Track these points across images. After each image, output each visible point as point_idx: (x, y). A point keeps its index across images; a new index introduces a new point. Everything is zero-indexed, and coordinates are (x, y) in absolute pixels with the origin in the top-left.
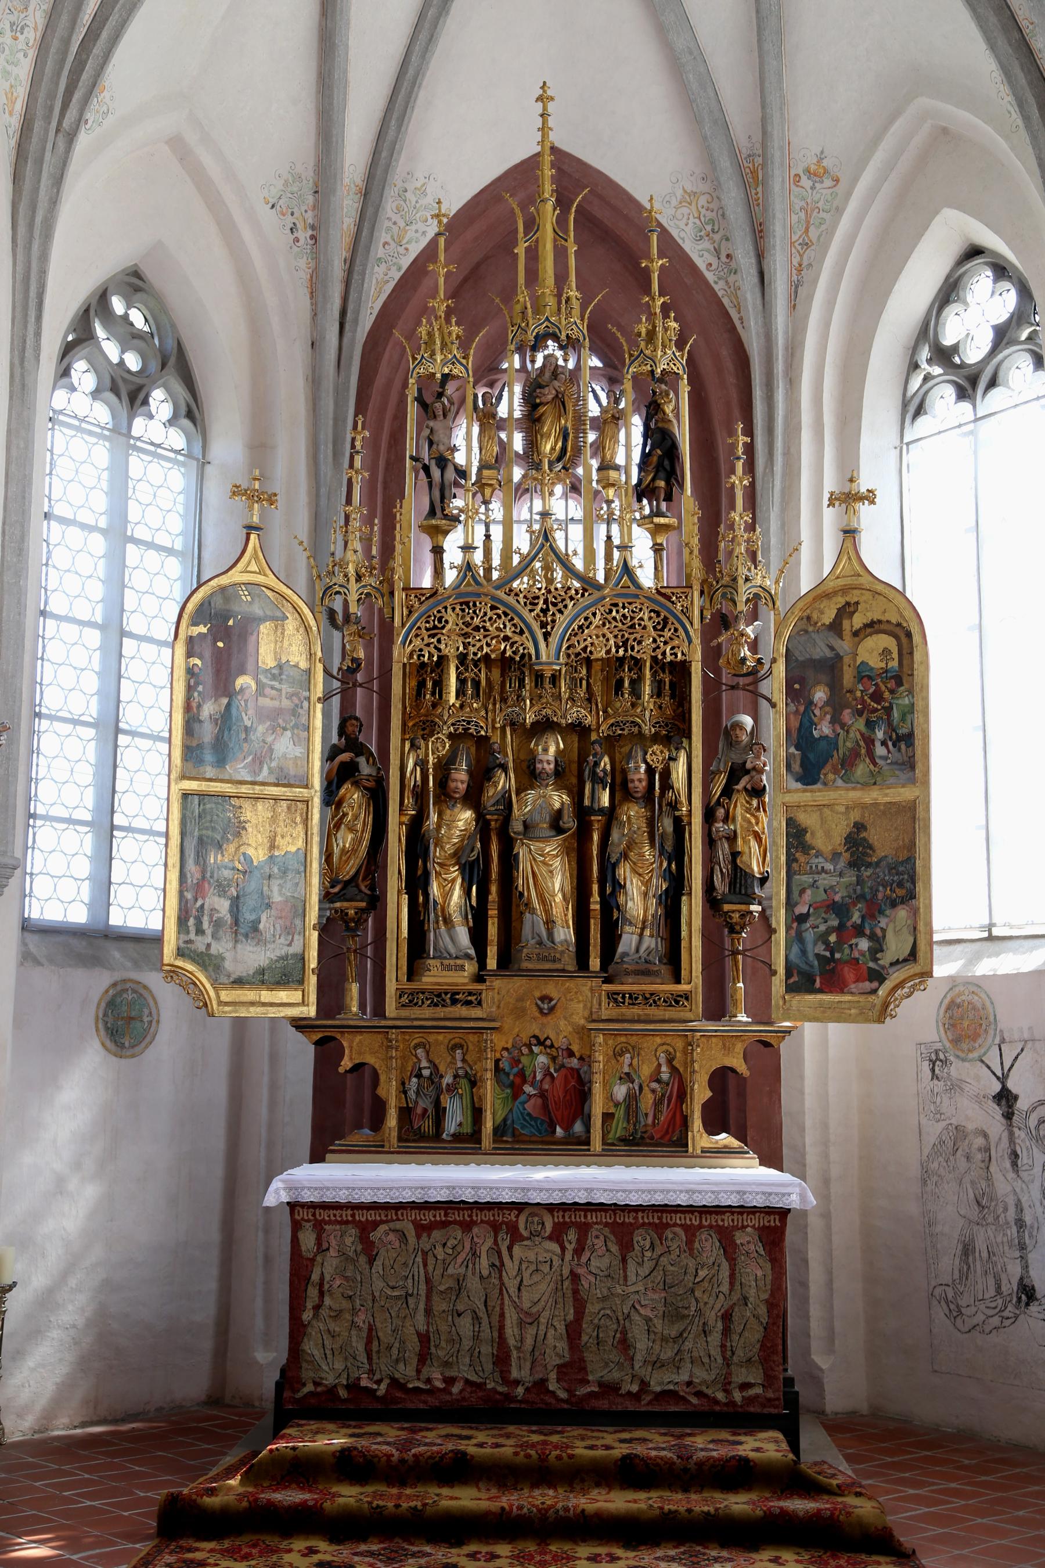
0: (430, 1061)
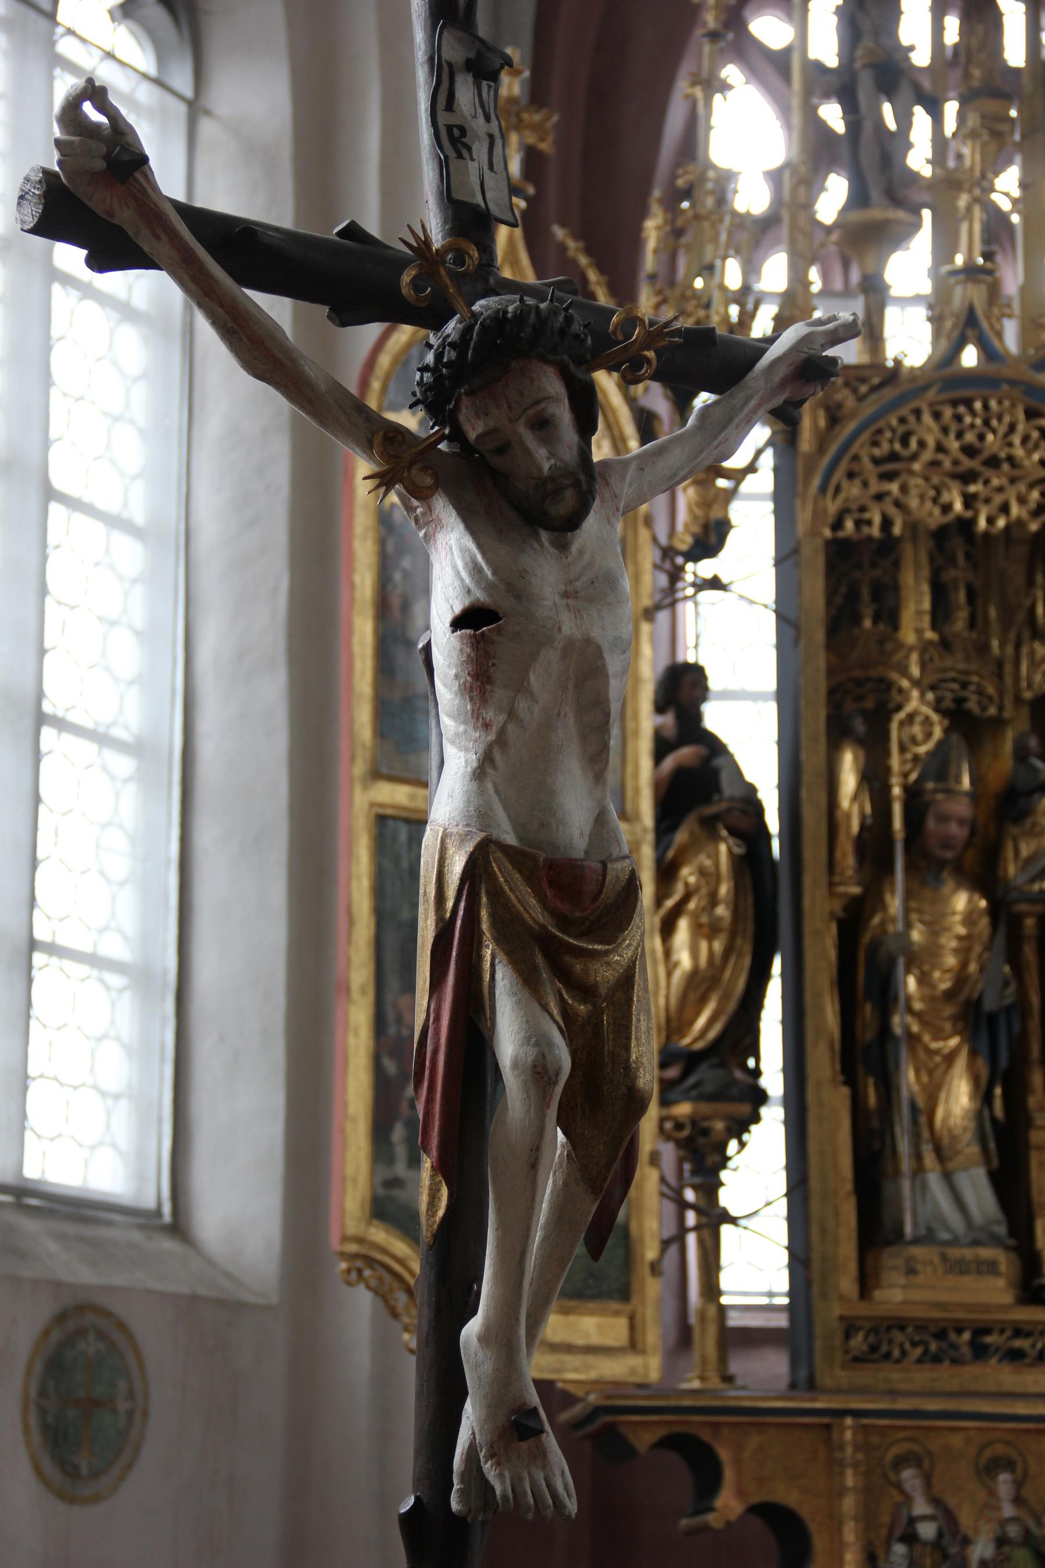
0: (935, 1501)
